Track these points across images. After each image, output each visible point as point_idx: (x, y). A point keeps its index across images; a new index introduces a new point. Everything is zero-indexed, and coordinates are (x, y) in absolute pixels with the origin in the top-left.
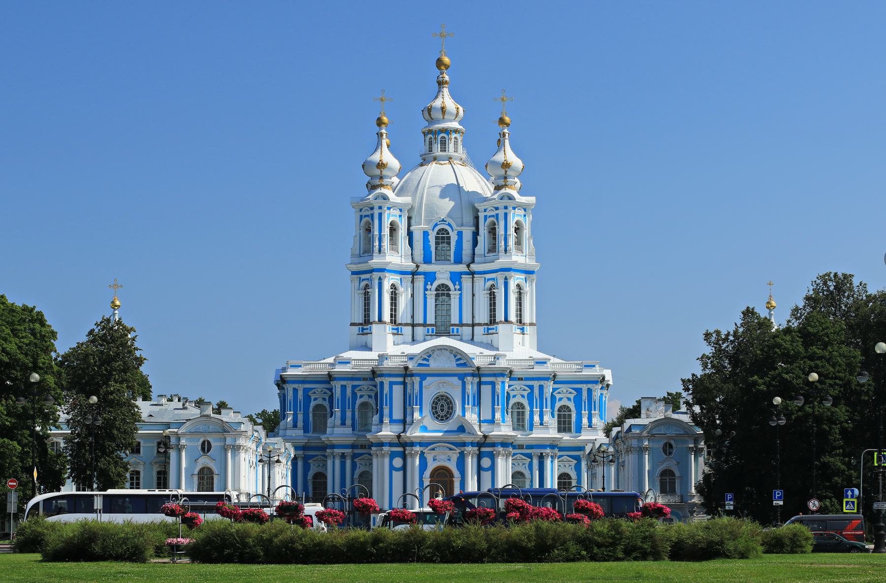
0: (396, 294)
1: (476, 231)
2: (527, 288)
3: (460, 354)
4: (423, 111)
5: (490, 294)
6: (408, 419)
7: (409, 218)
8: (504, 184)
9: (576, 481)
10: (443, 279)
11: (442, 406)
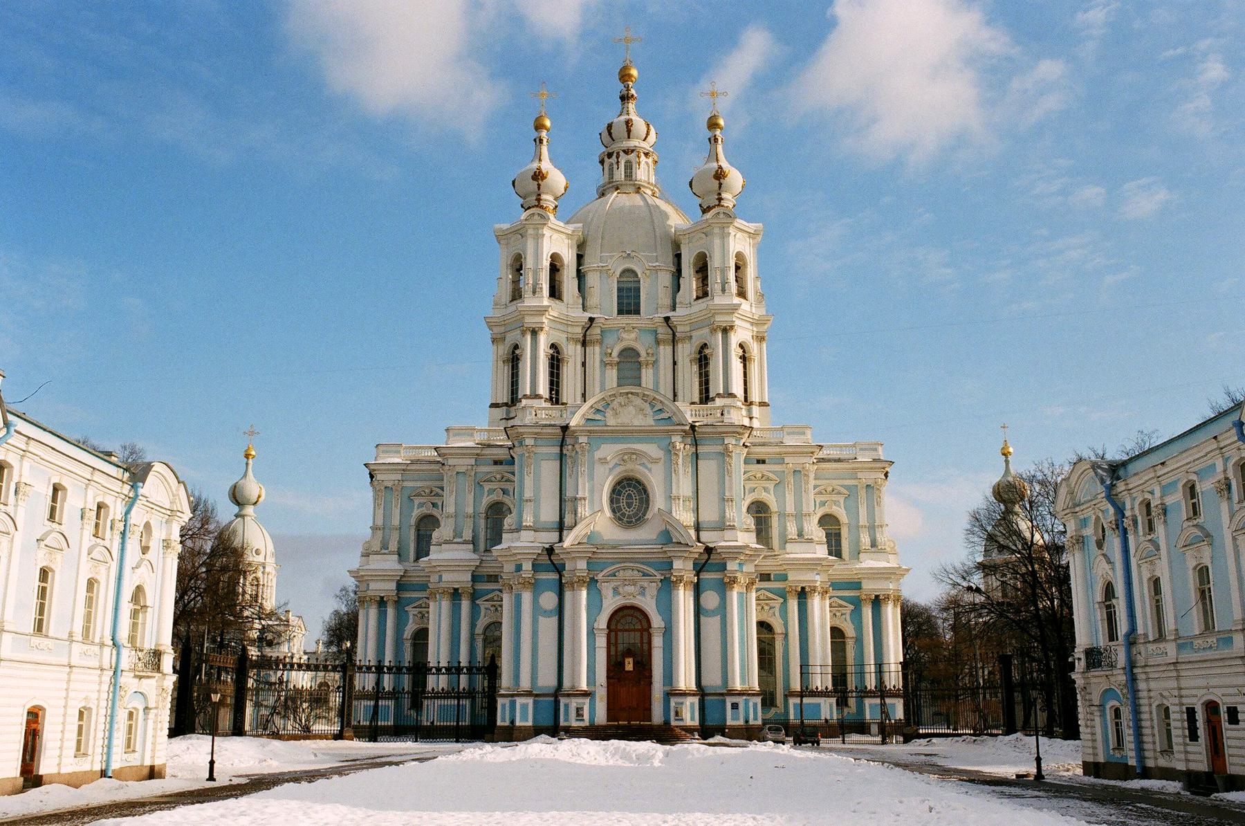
0: (558, 360)
1: (677, 275)
2: (754, 348)
3: (661, 402)
4: (600, 134)
5: (700, 360)
6: (568, 520)
7: (580, 258)
8: (717, 203)
9: (854, 640)
10: (629, 339)
11: (629, 496)
